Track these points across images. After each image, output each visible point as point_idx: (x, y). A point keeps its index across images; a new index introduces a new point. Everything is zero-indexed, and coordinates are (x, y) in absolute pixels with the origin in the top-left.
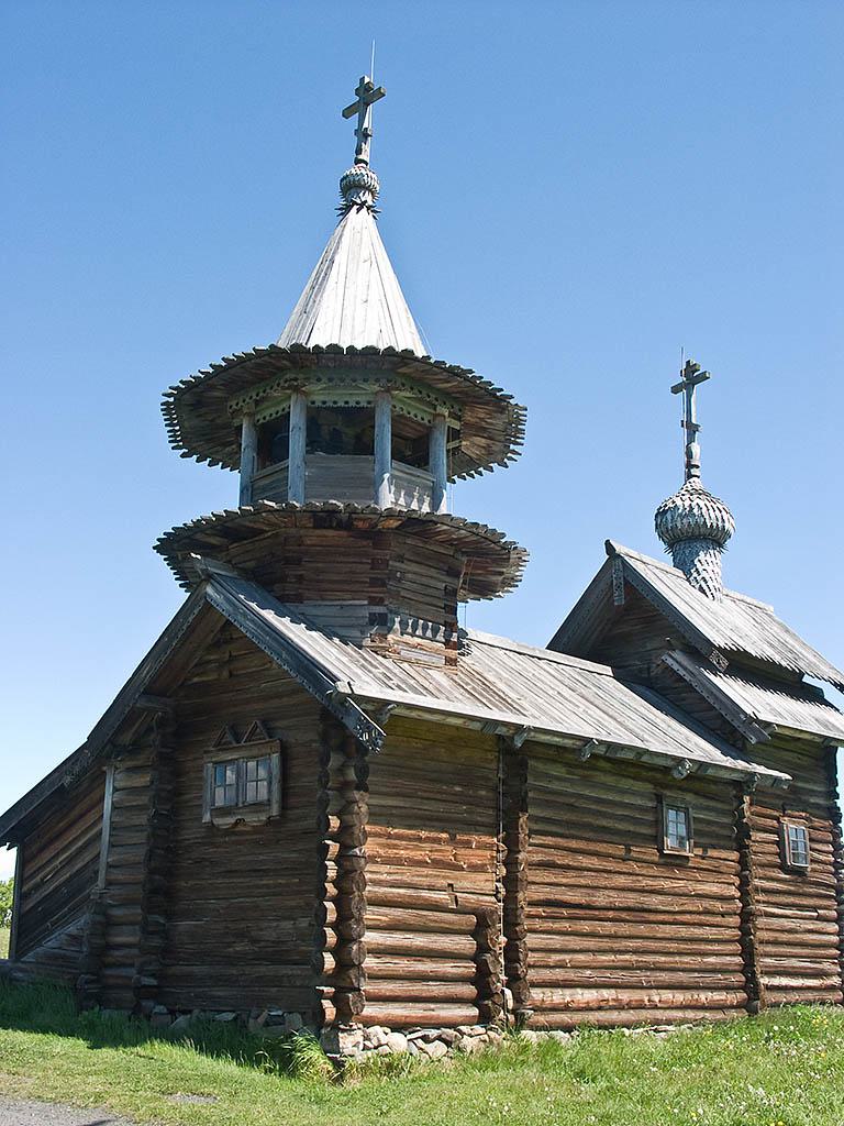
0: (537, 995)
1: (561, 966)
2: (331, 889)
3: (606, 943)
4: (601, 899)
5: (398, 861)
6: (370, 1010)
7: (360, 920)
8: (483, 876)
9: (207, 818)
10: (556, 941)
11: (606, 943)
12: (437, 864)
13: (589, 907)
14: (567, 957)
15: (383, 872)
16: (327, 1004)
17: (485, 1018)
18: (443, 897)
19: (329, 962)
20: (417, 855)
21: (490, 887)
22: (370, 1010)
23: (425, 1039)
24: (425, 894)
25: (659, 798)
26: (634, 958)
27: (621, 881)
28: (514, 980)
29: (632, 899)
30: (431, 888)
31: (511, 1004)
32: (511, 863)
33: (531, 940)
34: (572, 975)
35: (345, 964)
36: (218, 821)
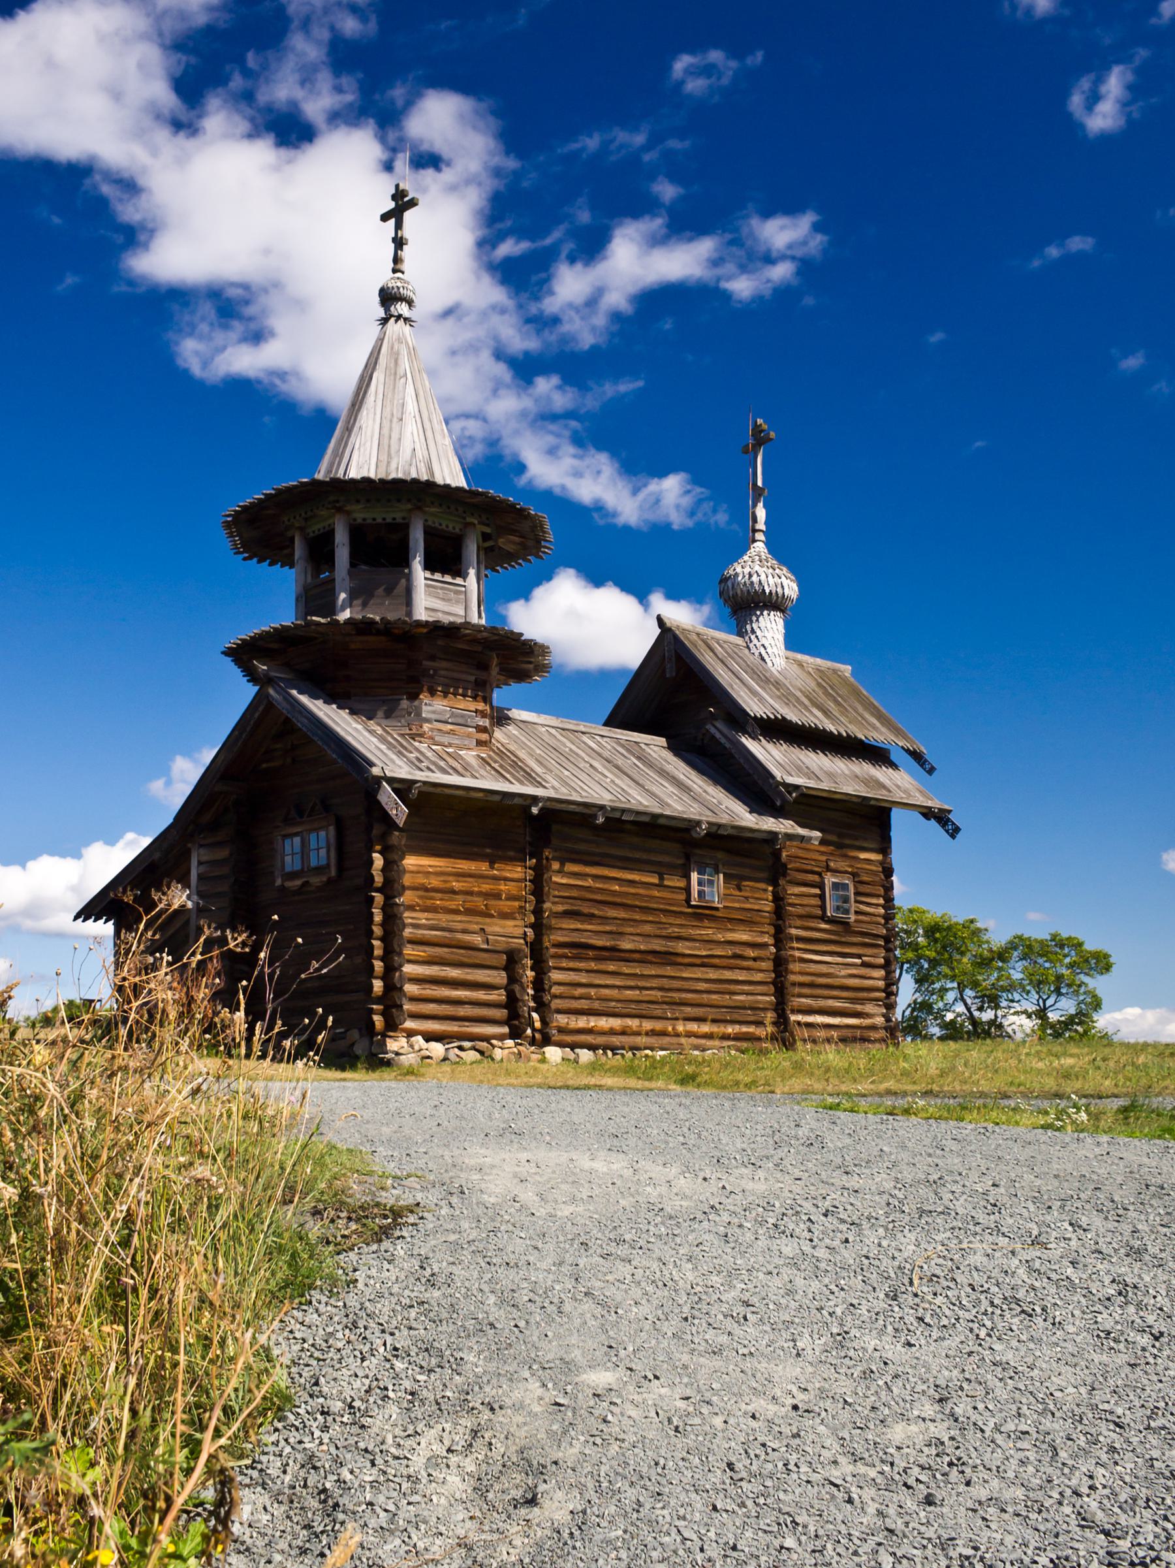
0: (562, 1020)
2: (377, 931)
4: (626, 945)
5: (434, 910)
6: (409, 1024)
7: (400, 954)
8: (510, 923)
9: (279, 882)
10: (583, 978)
12: (470, 912)
14: (592, 992)
15: (423, 918)
16: (376, 1018)
17: (516, 1034)
18: (477, 940)
19: (378, 985)
20: (452, 905)
21: (519, 931)
22: (409, 1024)
23: (461, 1048)
24: (459, 936)
25: (688, 857)
26: (660, 994)
27: (648, 928)
28: (541, 1006)
29: (657, 945)
30: (464, 931)
31: (538, 1025)
32: (538, 912)
33: (555, 976)
34: (596, 1005)
35: (392, 988)
36: (288, 884)
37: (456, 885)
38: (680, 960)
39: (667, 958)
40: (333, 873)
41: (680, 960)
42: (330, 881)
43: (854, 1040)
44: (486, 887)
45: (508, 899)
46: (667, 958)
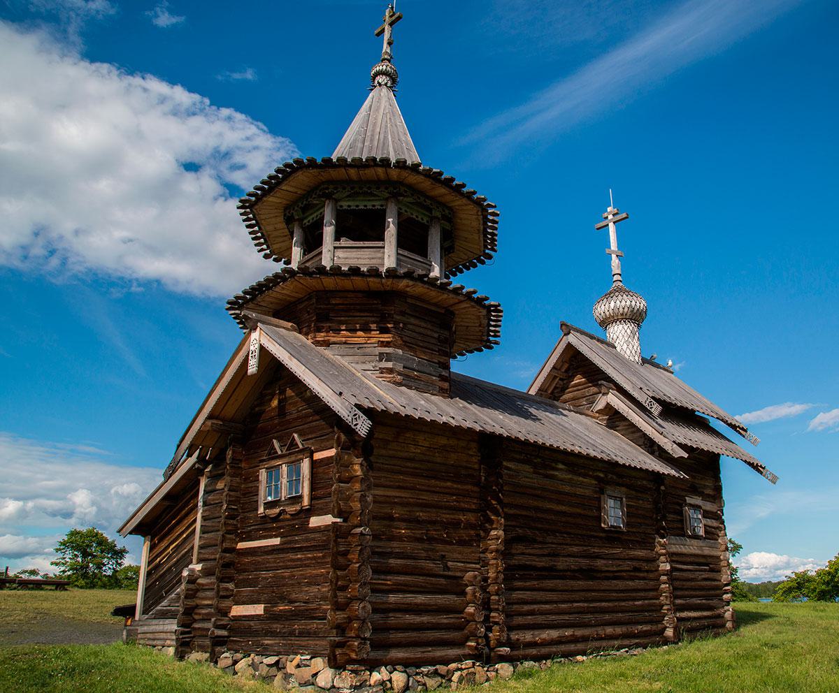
1: (532, 613)
3: (565, 596)
4: (561, 564)
11: (565, 596)
13: (551, 569)
14: (535, 607)
27: (575, 549)
29: (584, 562)
34: (540, 619)
37: (422, 515)
38: (599, 575)
39: (590, 574)
40: (306, 501)
41: (599, 575)
42: (301, 511)
43: (703, 628)
44: (446, 517)
45: (465, 528)
46: (590, 574)
